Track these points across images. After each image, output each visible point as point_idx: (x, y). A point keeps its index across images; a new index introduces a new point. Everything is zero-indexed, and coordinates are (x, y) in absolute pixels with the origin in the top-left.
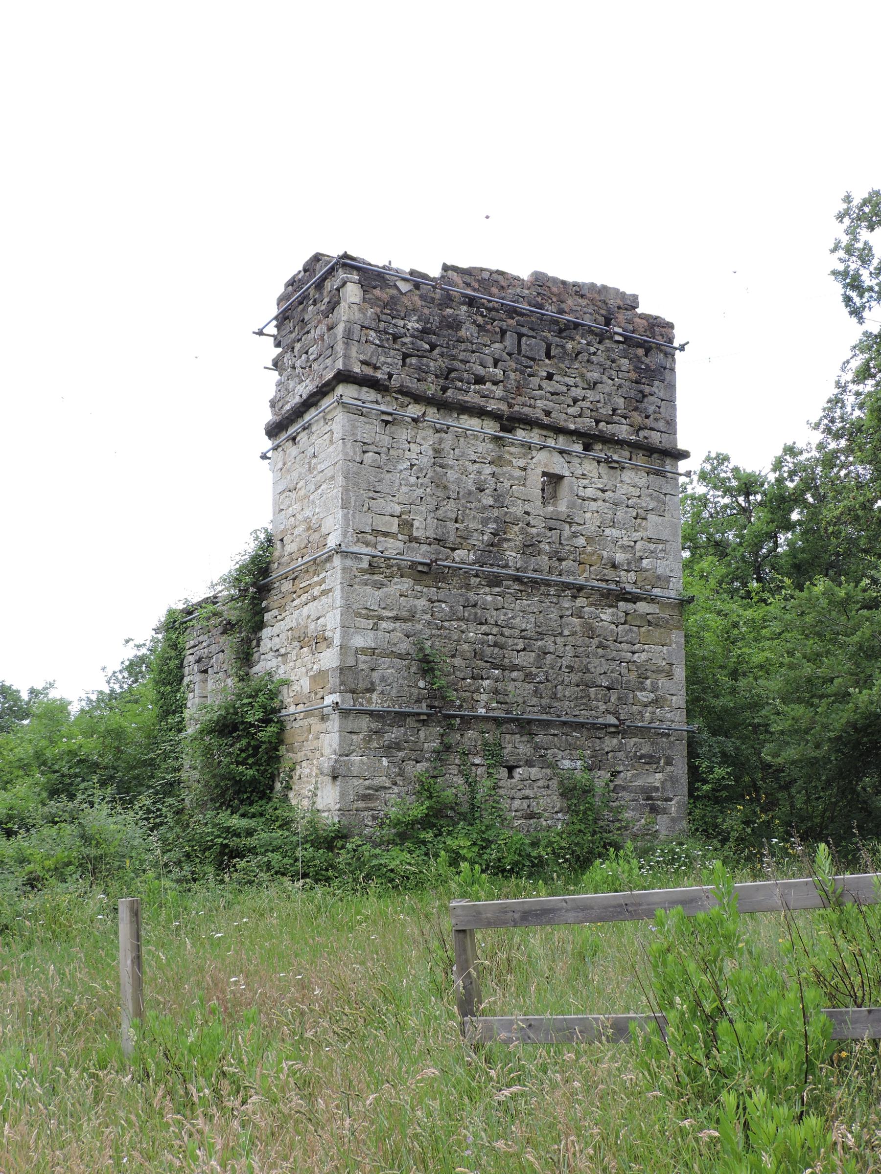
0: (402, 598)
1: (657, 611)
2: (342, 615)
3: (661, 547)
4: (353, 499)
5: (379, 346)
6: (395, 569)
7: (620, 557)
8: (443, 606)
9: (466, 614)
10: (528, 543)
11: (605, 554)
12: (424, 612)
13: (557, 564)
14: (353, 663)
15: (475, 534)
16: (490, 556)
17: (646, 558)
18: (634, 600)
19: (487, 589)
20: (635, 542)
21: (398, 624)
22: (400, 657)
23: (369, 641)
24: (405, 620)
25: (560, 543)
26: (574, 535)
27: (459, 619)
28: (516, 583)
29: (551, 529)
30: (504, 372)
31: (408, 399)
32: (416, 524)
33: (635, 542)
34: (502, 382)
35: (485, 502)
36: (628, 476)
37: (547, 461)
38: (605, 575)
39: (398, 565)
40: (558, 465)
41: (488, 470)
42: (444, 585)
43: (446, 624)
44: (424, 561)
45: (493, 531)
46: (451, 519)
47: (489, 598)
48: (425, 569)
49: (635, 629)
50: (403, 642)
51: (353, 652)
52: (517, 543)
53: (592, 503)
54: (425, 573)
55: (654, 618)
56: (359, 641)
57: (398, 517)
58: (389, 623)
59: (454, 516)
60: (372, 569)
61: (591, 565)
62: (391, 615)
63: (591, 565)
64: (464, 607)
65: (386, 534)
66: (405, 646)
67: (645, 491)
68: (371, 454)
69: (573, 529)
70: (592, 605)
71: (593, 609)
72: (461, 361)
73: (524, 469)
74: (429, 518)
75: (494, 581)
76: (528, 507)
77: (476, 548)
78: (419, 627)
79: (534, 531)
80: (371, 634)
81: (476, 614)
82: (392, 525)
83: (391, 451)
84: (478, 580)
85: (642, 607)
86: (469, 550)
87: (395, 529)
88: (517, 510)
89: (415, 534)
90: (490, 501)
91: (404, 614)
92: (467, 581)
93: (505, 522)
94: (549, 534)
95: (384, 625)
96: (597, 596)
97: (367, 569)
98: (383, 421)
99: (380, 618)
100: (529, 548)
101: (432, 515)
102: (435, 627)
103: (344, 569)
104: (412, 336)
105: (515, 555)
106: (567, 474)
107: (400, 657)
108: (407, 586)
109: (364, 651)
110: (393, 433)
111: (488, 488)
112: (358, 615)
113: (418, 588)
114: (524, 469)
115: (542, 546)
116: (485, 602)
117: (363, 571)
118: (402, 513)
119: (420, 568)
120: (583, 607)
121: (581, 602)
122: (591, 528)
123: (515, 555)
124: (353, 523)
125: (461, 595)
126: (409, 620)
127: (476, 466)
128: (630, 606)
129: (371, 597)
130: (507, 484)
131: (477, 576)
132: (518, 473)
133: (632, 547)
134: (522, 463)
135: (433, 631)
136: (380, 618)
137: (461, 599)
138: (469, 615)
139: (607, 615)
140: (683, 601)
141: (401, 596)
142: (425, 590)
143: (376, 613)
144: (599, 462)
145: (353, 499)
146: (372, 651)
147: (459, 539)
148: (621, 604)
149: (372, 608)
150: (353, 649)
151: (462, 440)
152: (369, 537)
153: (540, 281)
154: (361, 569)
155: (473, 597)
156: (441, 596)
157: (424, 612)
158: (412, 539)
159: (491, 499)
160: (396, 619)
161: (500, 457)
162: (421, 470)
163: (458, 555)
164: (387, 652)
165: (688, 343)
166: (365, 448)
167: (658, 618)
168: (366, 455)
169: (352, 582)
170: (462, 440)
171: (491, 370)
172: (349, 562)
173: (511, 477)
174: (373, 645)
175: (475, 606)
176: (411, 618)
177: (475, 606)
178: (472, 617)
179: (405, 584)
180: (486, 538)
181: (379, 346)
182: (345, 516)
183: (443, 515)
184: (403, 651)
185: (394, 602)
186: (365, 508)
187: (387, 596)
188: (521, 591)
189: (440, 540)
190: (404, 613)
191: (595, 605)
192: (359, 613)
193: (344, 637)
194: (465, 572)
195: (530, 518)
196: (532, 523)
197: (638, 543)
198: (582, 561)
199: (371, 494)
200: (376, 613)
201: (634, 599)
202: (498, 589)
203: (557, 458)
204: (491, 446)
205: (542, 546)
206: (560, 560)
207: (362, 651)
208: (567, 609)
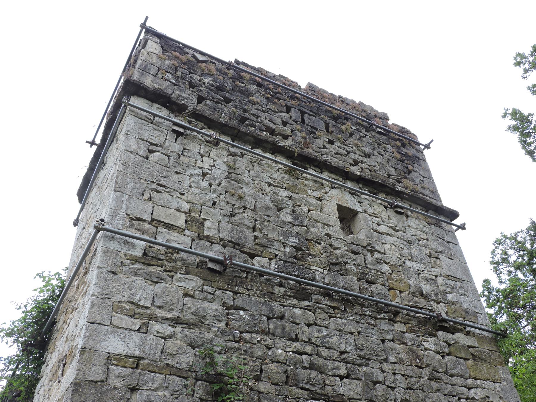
0: (187, 299)
1: (476, 345)
2: (92, 306)
3: (459, 284)
4: (130, 186)
5: (175, 85)
6: (179, 264)
7: (426, 288)
8: (242, 313)
9: (271, 327)
10: (334, 261)
11: (411, 282)
12: (217, 318)
13: (366, 285)
14: (100, 376)
15: (275, 243)
16: (294, 267)
17: (449, 292)
18: (451, 330)
19: (295, 301)
20: (436, 276)
21: (178, 329)
22: (180, 373)
23: (132, 346)
24: (189, 325)
25: (366, 267)
26: (379, 262)
27: (262, 332)
28: (327, 298)
29: (355, 253)
30: (292, 131)
31: (203, 124)
32: (207, 224)
33: (436, 276)
34: (291, 136)
35: (284, 218)
36: (412, 222)
37: (338, 196)
38: (416, 302)
39: (184, 261)
40: (351, 202)
41: (284, 193)
42: (241, 290)
43: (247, 336)
44: (217, 257)
45: (295, 245)
46: (248, 227)
47: (298, 311)
48: (218, 268)
49: (462, 361)
50: (184, 353)
51: (103, 360)
52: (323, 260)
53: (388, 237)
54: (216, 272)
55: (476, 351)
56: (116, 345)
57: (185, 213)
58: (165, 326)
59: (251, 225)
60: (147, 258)
61: (401, 292)
62: (169, 316)
63: (401, 292)
64: (269, 318)
65: (169, 227)
66: (187, 359)
67: (429, 237)
68: (157, 154)
69: (375, 256)
70: (412, 331)
71: (413, 336)
72: (253, 115)
73: (320, 199)
74: (223, 222)
75: (302, 294)
76: (329, 230)
77: (278, 257)
78: (209, 336)
79: (338, 252)
80: (136, 337)
81: (284, 327)
82: (178, 219)
83: (182, 157)
84: (283, 290)
85: (460, 337)
86: (270, 259)
87: (181, 222)
88: (318, 231)
89: (206, 233)
90: (290, 219)
91: (188, 317)
92: (270, 289)
93: (307, 239)
94: (354, 257)
95: (157, 327)
96: (414, 322)
97: (140, 258)
98: (174, 131)
99: (152, 318)
100: (335, 265)
101: (227, 219)
102: (231, 338)
103: (106, 252)
104: (206, 87)
105: (322, 270)
106: (360, 210)
107: (180, 373)
108: (193, 284)
109: (121, 360)
110: (184, 144)
111: (285, 207)
112: (118, 309)
113: (209, 289)
114: (320, 199)
115: (348, 266)
116: (292, 315)
117: (134, 260)
118: (190, 211)
119: (211, 265)
120: (404, 333)
121: (399, 327)
122: (393, 256)
123: (322, 270)
124: (127, 206)
125: (263, 304)
126: (195, 325)
127: (272, 188)
128: (449, 336)
129: (143, 291)
130: (305, 208)
131: (281, 285)
132: (313, 201)
133: (434, 280)
134: (316, 194)
135: (229, 344)
136: (152, 318)
137: (263, 308)
138: (276, 328)
139: (429, 343)
140: (497, 334)
141: (185, 295)
142: (218, 292)
143: (148, 311)
144: (386, 207)
145: (130, 186)
146: (136, 362)
147: (258, 247)
148: (440, 333)
149: (142, 303)
150: (105, 356)
151: (256, 165)
152: (147, 226)
153: (311, 88)
154: (131, 255)
155: (278, 308)
156: (239, 302)
157: (217, 318)
158: (201, 237)
159: (290, 217)
160: (176, 322)
161: (295, 186)
162: (214, 179)
163: (258, 262)
164: (160, 364)
165: (432, 141)
166: (151, 148)
167: (480, 351)
168: (152, 155)
169: (117, 270)
170: (256, 165)
171: (280, 126)
172: (114, 246)
173: (307, 203)
174: (137, 353)
175: (282, 317)
176: (199, 322)
177: (282, 317)
178: (279, 331)
179: (193, 283)
180: (287, 250)
181: (175, 85)
182: (118, 200)
183: (238, 221)
184: (184, 366)
185: (175, 301)
186: (147, 196)
187: (166, 293)
188: (334, 308)
189: (235, 244)
190: (188, 317)
191: (415, 331)
192: (121, 308)
193: (90, 336)
194: (268, 280)
195: (332, 240)
196: (335, 244)
197: (439, 278)
198: (391, 286)
199: (154, 186)
200: (148, 311)
201: (452, 330)
202: (306, 303)
203: (349, 197)
204: (286, 176)
205: (348, 266)
206: (370, 282)
207: (117, 360)
208: (387, 332)
